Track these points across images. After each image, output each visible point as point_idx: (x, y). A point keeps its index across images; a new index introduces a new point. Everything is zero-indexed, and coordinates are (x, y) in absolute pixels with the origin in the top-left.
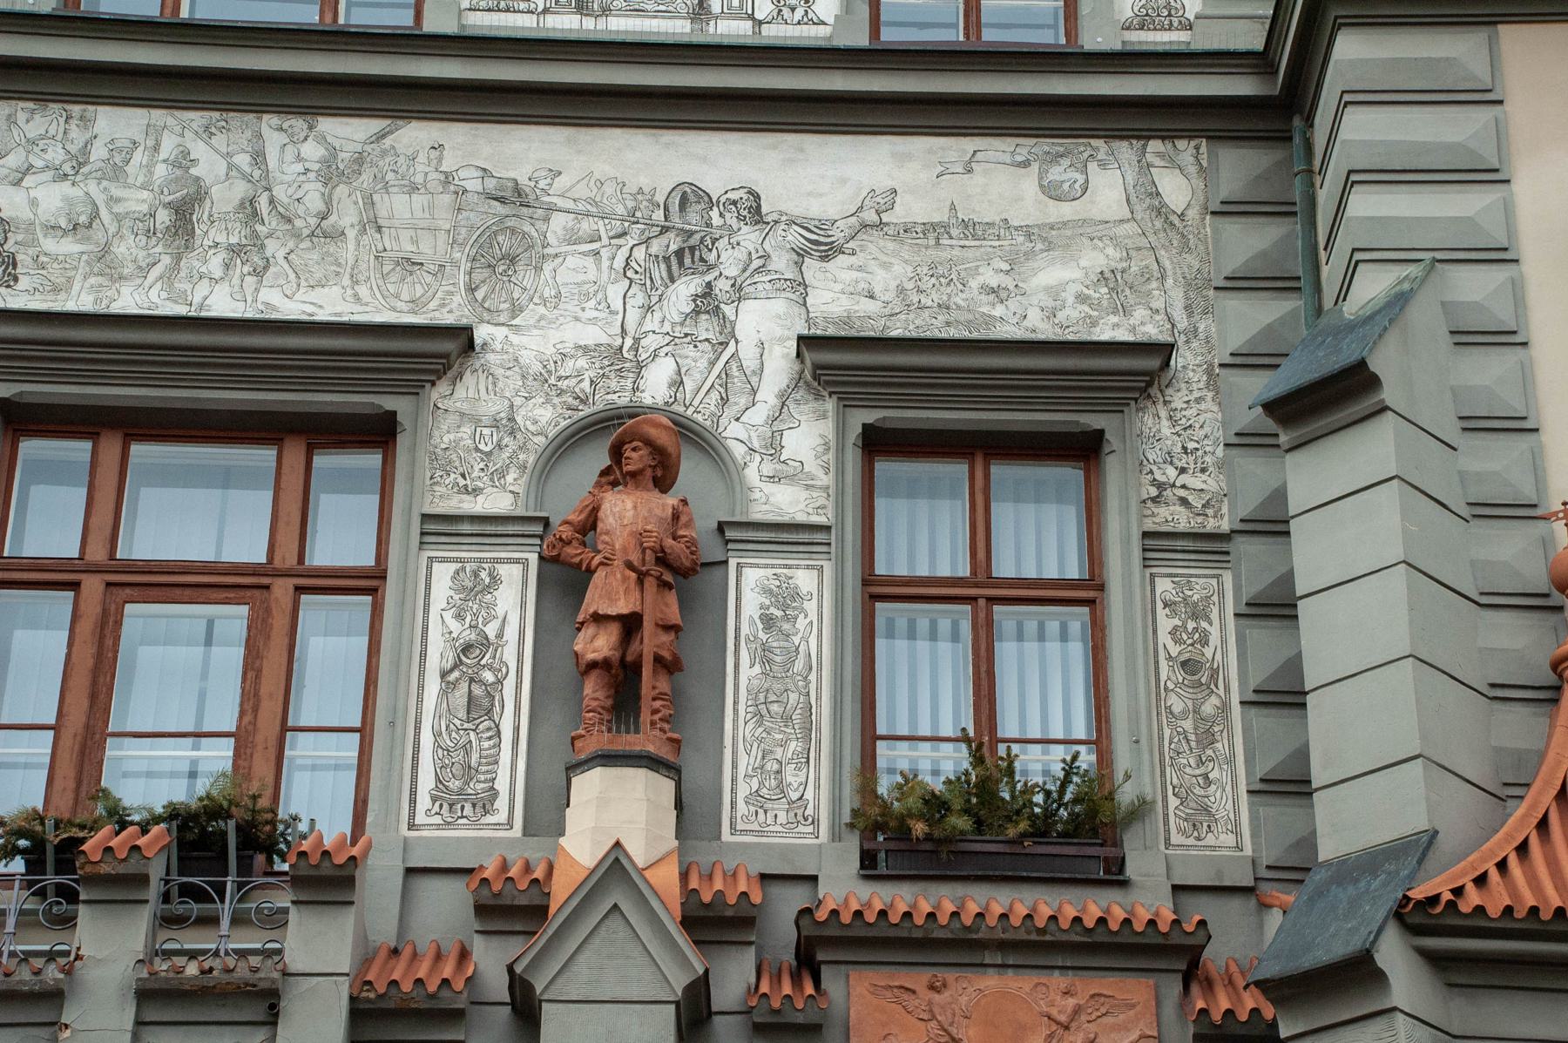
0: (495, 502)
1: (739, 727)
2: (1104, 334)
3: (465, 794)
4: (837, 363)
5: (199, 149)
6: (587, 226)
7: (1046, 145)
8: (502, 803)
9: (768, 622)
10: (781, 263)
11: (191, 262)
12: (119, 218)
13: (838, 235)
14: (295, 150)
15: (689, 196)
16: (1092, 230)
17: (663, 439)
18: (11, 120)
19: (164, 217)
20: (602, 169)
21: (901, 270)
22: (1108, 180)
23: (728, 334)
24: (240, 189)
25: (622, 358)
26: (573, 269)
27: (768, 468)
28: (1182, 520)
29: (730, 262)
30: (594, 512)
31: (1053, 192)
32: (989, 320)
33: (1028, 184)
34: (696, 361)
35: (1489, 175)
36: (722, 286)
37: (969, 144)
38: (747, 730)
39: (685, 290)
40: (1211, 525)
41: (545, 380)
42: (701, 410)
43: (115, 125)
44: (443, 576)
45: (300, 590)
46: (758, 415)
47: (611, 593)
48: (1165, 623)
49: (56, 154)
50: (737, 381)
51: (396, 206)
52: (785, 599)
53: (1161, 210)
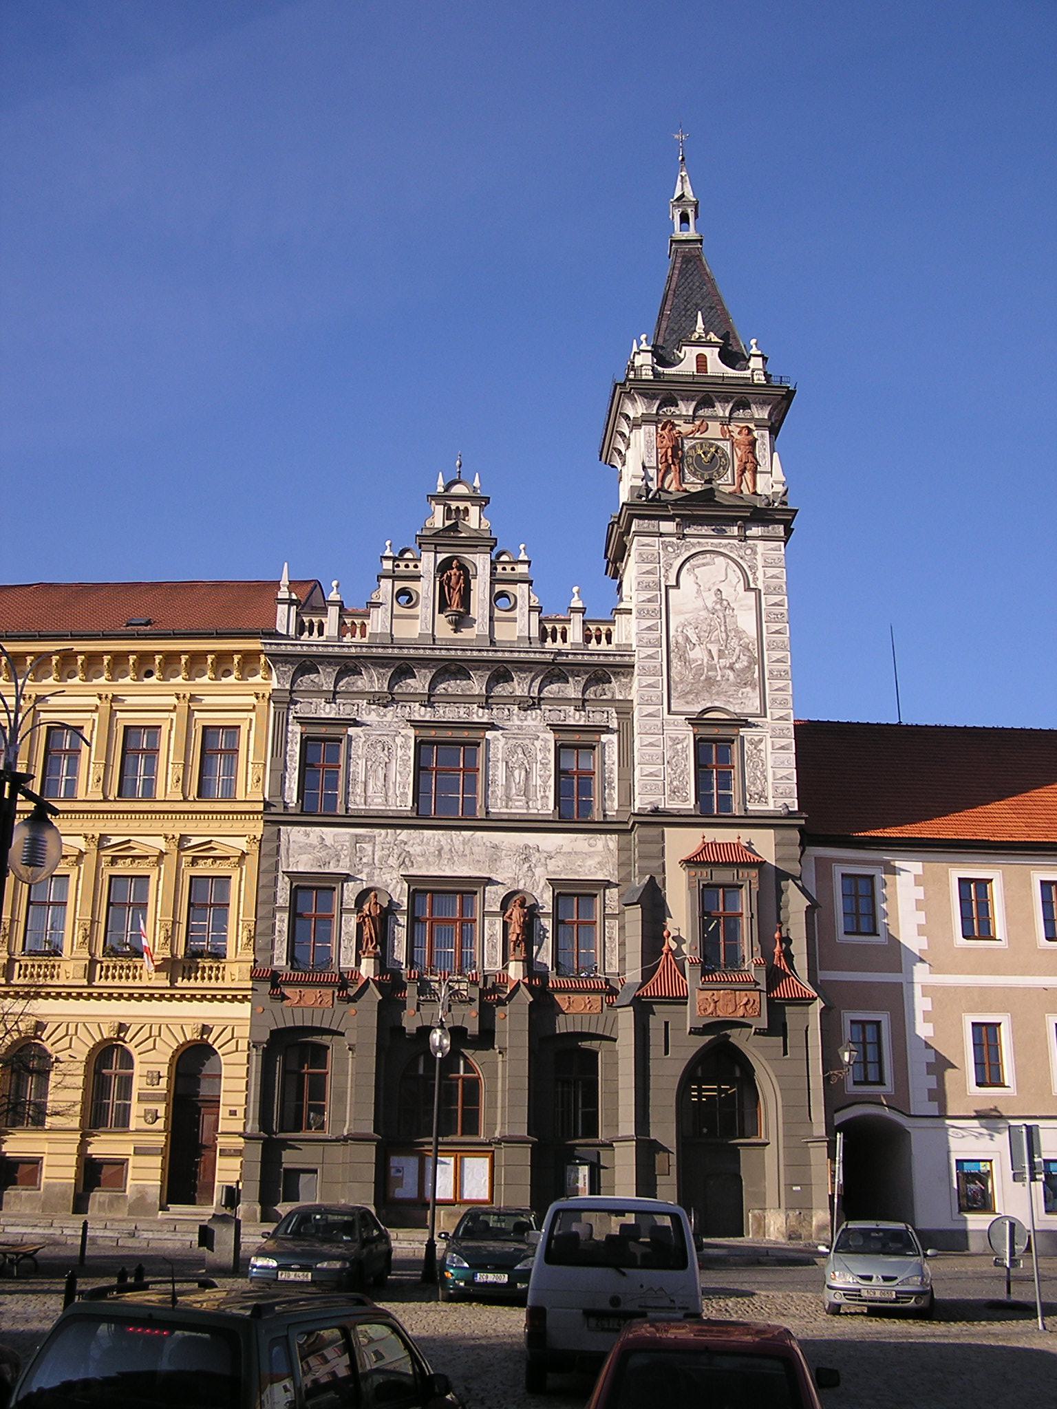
15: (526, 847)
25: (515, 880)
26: (506, 862)
34: (528, 879)
39: (527, 865)
51: (476, 849)
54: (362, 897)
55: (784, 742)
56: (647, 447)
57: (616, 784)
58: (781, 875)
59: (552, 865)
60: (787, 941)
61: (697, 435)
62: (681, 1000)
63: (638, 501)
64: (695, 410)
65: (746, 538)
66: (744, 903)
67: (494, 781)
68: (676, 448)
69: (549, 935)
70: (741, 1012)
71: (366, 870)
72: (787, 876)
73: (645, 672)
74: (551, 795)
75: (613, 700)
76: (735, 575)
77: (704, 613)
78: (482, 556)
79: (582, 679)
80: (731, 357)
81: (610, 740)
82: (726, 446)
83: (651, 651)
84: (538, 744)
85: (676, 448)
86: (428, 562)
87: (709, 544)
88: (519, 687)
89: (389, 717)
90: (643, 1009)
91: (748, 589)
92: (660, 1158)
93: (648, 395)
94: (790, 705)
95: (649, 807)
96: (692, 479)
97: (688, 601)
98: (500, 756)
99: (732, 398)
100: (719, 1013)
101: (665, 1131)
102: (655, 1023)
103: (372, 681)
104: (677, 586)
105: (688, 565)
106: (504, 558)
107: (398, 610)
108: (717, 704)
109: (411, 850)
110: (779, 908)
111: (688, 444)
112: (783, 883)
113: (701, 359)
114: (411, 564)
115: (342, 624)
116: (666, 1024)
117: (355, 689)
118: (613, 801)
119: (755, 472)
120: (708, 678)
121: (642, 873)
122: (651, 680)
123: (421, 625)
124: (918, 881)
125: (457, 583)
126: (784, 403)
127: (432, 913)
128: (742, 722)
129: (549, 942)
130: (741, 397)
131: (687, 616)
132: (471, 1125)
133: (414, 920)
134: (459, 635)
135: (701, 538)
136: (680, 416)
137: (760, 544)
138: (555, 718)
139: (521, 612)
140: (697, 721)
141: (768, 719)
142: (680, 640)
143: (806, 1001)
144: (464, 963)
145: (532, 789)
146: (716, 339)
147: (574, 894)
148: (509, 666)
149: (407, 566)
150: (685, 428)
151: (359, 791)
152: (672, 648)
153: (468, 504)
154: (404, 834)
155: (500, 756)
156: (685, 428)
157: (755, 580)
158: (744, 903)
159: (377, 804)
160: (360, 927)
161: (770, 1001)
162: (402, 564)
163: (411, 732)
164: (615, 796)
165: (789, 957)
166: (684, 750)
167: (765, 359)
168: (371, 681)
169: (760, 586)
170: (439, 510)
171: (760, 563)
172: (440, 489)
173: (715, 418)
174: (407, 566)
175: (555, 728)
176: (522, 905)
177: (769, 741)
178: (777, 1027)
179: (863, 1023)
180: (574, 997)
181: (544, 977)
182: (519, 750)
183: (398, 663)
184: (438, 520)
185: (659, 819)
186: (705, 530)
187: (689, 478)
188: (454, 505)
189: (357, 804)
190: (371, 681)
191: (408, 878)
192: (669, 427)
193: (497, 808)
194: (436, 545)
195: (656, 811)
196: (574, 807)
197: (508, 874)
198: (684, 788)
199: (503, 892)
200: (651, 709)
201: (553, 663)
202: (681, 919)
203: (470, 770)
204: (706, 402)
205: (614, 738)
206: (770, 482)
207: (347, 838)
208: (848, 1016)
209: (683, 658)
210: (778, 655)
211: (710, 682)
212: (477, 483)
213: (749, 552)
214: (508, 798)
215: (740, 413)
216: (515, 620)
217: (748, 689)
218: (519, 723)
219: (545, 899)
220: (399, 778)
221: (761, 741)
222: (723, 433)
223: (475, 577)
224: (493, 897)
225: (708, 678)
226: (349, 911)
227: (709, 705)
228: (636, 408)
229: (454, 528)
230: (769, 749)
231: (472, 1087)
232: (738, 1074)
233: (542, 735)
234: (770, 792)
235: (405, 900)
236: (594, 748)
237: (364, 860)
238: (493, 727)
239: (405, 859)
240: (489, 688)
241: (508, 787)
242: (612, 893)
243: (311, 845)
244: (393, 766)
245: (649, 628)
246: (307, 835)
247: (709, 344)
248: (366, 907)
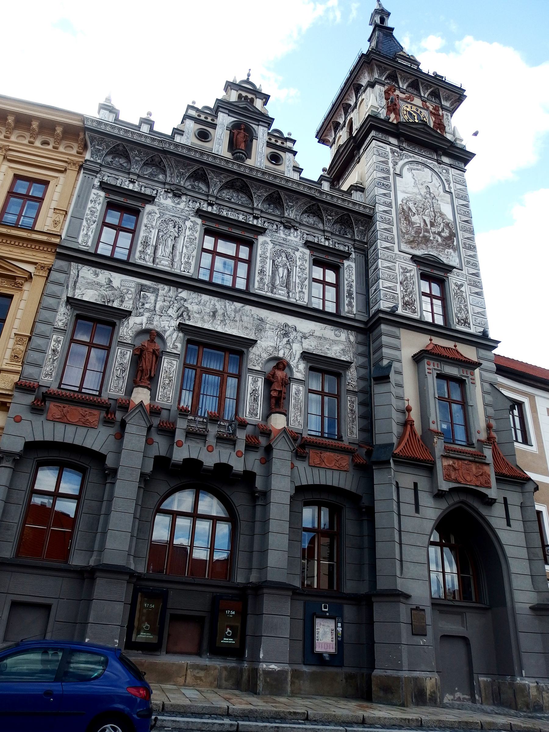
0: (258, 368)
1: (291, 409)
2: (342, 359)
3: (253, 413)
5: (217, 304)
6: (272, 327)
7: (335, 328)
8: (258, 415)
9: (296, 394)
10: (299, 338)
11: (215, 321)
12: (205, 312)
13: (307, 335)
14: (232, 307)
15: (286, 325)
16: (340, 342)
17: (285, 364)
18: (190, 294)
19: (211, 313)
20: (274, 318)
21: (315, 343)
22: (344, 335)
23: (291, 348)
24: (222, 311)
25: (276, 349)
26: (270, 333)
27: (296, 370)
28: (351, 389)
29: (292, 336)
30: (274, 373)
31: (336, 335)
32: (327, 353)
34: (287, 351)
35: (398, 349)
36: (291, 340)
37: (325, 325)
38: (293, 410)
39: (285, 340)
40: (355, 390)
41: (265, 350)
42: (288, 359)
43: (205, 298)
44: (250, 378)
45: (228, 376)
46: (295, 361)
47: (276, 387)
48: (349, 404)
49: (196, 301)
50: (292, 356)
51: (245, 318)
52: (298, 391)
53: (350, 341)
61: (409, 101)
71: (147, 315)
76: (436, 182)
77: (419, 197)
84: (298, 254)
86: (224, 120)
87: (420, 159)
89: (182, 205)
99: (431, 87)
109: (190, 307)
117: (156, 179)
120: (424, 237)
128: (449, 269)
131: (409, 195)
141: (463, 272)
151: (149, 252)
154: (184, 294)
155: (268, 255)
159: (164, 264)
169: (453, 191)
182: (284, 255)
188: (244, 94)
191: (182, 327)
198: (413, 304)
207: (133, 285)
211: (426, 240)
213: (444, 171)
214: (273, 286)
217: (451, 250)
218: (284, 236)
221: (462, 285)
233: (301, 249)
234: (471, 320)
237: (147, 306)
239: (183, 312)
243: (98, 284)
244: (181, 241)
246: (97, 275)
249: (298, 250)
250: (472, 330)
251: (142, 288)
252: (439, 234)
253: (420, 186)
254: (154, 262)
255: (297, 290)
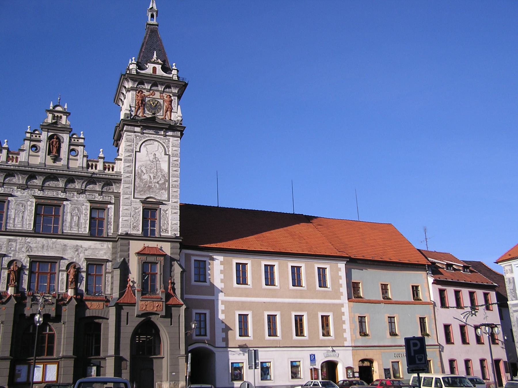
4: (87, 259)
15: (77, 246)
16: (104, 249)
25: (72, 258)
26: (69, 251)
29: (80, 251)
33: (100, 245)
42: (77, 262)
43: (39, 239)
51: (57, 246)
54: (10, 263)
55: (175, 211)
56: (132, 99)
57: (112, 223)
58: (172, 260)
59: (87, 253)
60: (173, 283)
61: (151, 96)
62: (133, 305)
63: (127, 119)
64: (151, 87)
65: (166, 136)
66: (158, 269)
67: (66, 220)
68: (143, 101)
69: (85, 279)
70: (155, 309)
71: (13, 253)
72: (174, 260)
73: (126, 182)
74: (88, 226)
75: (113, 193)
76: (161, 149)
77: (149, 162)
78: (66, 135)
79: (102, 184)
80: (166, 69)
81: (111, 207)
82: (161, 101)
83: (128, 175)
85: (143, 101)
86: (44, 135)
87: (152, 137)
88: (77, 185)
89: (25, 194)
90: (119, 307)
91: (166, 154)
92: (123, 363)
93: (134, 80)
94: (179, 198)
95: (124, 233)
96: (148, 112)
97: (143, 157)
98: (69, 211)
100: (147, 309)
101: (126, 353)
102: (123, 313)
103: (19, 180)
104: (140, 151)
105: (144, 144)
106: (75, 136)
107: (31, 153)
108: (152, 196)
109: (31, 245)
110: (171, 272)
111: (147, 99)
112: (173, 262)
113: (154, 69)
114: (38, 136)
115: (8, 157)
116: (128, 313)
118: (111, 230)
119: (171, 112)
120: (149, 186)
121: (121, 257)
122: (128, 185)
123: (40, 159)
124: (222, 263)
125: (56, 144)
126: (184, 87)
127: (39, 270)
128: (161, 203)
129: (84, 282)
130: (168, 84)
132: (50, 352)
133: (31, 272)
134: (55, 164)
135: (150, 134)
136: (145, 89)
137: (171, 138)
138: (91, 198)
139: (80, 157)
140: (144, 202)
141: (170, 202)
142: (139, 171)
143: (179, 306)
144: (51, 289)
145: (80, 224)
146: (160, 62)
147: (95, 265)
148: (74, 177)
149: (36, 136)
150: (146, 93)
151: (11, 222)
152: (136, 174)
153: (62, 115)
154: (29, 239)
155: (69, 211)
156: (146, 93)
157: (169, 151)
158: (158, 269)
159: (18, 227)
160: (9, 275)
161: (167, 306)
162: (34, 135)
163: (34, 200)
164: (112, 228)
165: (174, 289)
166: (139, 212)
167: (178, 71)
168: (19, 179)
169: (170, 154)
170: (50, 116)
171: (171, 145)
172: (51, 108)
173: (158, 91)
174: (36, 136)
175: (91, 201)
176: (75, 268)
177: (170, 210)
178: (169, 315)
179: (200, 314)
180: (93, 303)
181: (82, 295)
182: (76, 209)
183: (30, 173)
184: (50, 119)
185: (128, 237)
186: (151, 132)
187: (147, 112)
188: (56, 114)
189: (10, 227)
190: (19, 179)
192: (141, 92)
193: (67, 231)
194: (48, 129)
195: (127, 234)
196: (96, 231)
197: (69, 256)
198: (138, 226)
199: (67, 262)
200: (127, 196)
201: (91, 177)
202: (134, 274)
203: (57, 216)
204: (155, 84)
205: (113, 206)
206: (176, 116)
207: (5, 240)
208: (194, 311)
209: (140, 178)
210: (175, 179)
211: (150, 187)
212: (66, 107)
213: (167, 141)
214: (71, 227)
215: (167, 90)
216: (77, 160)
217: (163, 191)
219: (84, 266)
220: (28, 218)
221: (167, 210)
222: (161, 96)
223: (63, 142)
224: (63, 264)
225: (149, 186)
226: (5, 268)
227: (149, 196)
228: (129, 85)
229: (56, 123)
230: (170, 213)
231: (52, 337)
232: (154, 332)
233: (85, 204)
234: (169, 229)
235: (28, 265)
236: (105, 210)
237: (12, 249)
238: (66, 200)
240: (66, 185)
241: (71, 223)
242: (109, 264)
244: (26, 213)
245: (128, 166)
247: (158, 63)
248: (12, 267)
249: (83, 205)
250: (170, 234)
251: (10, 241)
252: (158, 183)
253: (150, 155)
254: (14, 227)
255: (83, 227)
